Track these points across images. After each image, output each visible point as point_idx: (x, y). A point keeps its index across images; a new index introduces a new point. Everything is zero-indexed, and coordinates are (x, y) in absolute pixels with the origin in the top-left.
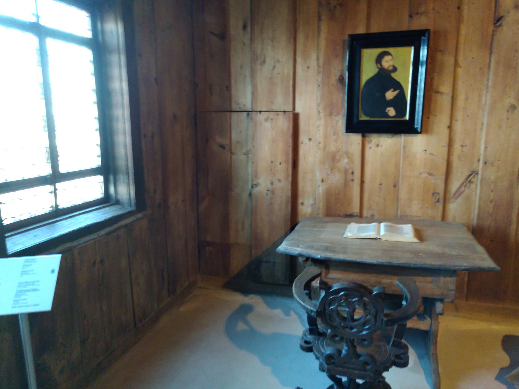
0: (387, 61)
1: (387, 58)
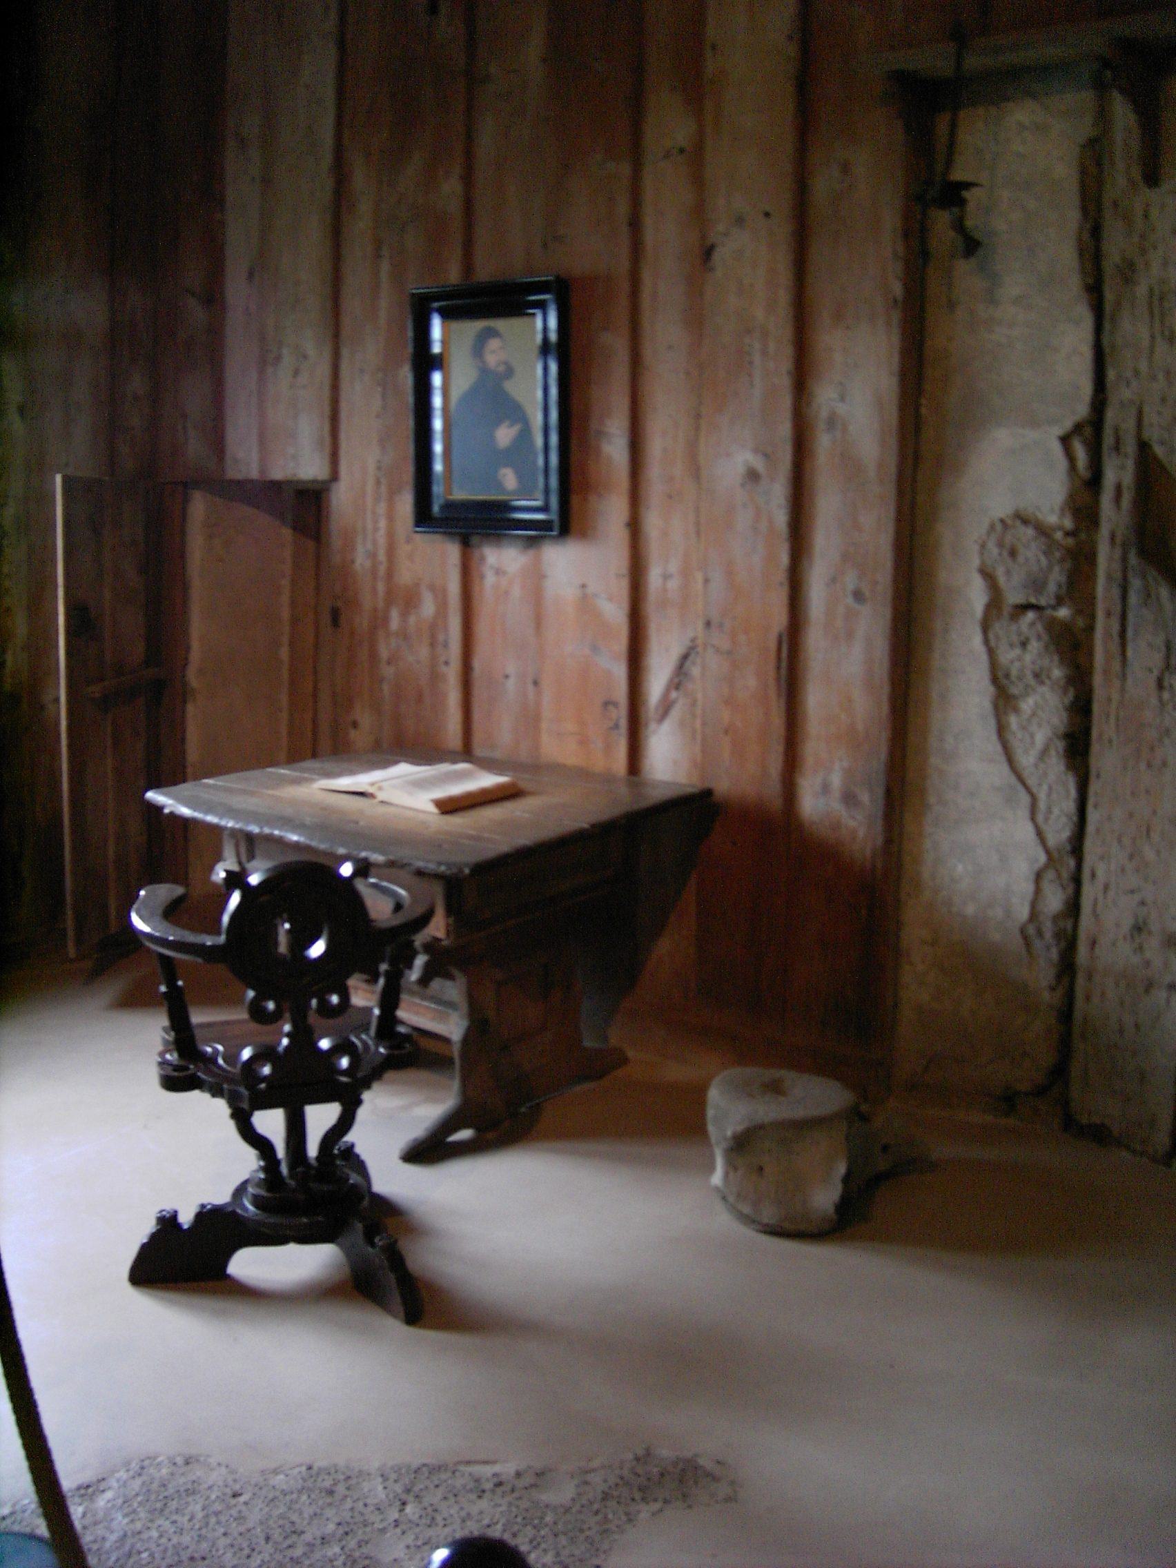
0: (493, 352)
1: (494, 344)
